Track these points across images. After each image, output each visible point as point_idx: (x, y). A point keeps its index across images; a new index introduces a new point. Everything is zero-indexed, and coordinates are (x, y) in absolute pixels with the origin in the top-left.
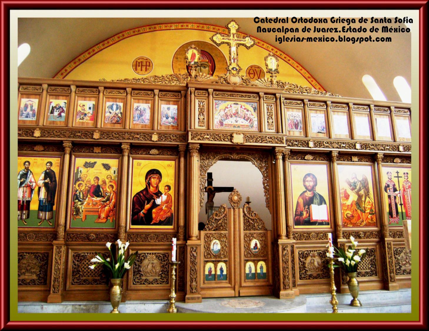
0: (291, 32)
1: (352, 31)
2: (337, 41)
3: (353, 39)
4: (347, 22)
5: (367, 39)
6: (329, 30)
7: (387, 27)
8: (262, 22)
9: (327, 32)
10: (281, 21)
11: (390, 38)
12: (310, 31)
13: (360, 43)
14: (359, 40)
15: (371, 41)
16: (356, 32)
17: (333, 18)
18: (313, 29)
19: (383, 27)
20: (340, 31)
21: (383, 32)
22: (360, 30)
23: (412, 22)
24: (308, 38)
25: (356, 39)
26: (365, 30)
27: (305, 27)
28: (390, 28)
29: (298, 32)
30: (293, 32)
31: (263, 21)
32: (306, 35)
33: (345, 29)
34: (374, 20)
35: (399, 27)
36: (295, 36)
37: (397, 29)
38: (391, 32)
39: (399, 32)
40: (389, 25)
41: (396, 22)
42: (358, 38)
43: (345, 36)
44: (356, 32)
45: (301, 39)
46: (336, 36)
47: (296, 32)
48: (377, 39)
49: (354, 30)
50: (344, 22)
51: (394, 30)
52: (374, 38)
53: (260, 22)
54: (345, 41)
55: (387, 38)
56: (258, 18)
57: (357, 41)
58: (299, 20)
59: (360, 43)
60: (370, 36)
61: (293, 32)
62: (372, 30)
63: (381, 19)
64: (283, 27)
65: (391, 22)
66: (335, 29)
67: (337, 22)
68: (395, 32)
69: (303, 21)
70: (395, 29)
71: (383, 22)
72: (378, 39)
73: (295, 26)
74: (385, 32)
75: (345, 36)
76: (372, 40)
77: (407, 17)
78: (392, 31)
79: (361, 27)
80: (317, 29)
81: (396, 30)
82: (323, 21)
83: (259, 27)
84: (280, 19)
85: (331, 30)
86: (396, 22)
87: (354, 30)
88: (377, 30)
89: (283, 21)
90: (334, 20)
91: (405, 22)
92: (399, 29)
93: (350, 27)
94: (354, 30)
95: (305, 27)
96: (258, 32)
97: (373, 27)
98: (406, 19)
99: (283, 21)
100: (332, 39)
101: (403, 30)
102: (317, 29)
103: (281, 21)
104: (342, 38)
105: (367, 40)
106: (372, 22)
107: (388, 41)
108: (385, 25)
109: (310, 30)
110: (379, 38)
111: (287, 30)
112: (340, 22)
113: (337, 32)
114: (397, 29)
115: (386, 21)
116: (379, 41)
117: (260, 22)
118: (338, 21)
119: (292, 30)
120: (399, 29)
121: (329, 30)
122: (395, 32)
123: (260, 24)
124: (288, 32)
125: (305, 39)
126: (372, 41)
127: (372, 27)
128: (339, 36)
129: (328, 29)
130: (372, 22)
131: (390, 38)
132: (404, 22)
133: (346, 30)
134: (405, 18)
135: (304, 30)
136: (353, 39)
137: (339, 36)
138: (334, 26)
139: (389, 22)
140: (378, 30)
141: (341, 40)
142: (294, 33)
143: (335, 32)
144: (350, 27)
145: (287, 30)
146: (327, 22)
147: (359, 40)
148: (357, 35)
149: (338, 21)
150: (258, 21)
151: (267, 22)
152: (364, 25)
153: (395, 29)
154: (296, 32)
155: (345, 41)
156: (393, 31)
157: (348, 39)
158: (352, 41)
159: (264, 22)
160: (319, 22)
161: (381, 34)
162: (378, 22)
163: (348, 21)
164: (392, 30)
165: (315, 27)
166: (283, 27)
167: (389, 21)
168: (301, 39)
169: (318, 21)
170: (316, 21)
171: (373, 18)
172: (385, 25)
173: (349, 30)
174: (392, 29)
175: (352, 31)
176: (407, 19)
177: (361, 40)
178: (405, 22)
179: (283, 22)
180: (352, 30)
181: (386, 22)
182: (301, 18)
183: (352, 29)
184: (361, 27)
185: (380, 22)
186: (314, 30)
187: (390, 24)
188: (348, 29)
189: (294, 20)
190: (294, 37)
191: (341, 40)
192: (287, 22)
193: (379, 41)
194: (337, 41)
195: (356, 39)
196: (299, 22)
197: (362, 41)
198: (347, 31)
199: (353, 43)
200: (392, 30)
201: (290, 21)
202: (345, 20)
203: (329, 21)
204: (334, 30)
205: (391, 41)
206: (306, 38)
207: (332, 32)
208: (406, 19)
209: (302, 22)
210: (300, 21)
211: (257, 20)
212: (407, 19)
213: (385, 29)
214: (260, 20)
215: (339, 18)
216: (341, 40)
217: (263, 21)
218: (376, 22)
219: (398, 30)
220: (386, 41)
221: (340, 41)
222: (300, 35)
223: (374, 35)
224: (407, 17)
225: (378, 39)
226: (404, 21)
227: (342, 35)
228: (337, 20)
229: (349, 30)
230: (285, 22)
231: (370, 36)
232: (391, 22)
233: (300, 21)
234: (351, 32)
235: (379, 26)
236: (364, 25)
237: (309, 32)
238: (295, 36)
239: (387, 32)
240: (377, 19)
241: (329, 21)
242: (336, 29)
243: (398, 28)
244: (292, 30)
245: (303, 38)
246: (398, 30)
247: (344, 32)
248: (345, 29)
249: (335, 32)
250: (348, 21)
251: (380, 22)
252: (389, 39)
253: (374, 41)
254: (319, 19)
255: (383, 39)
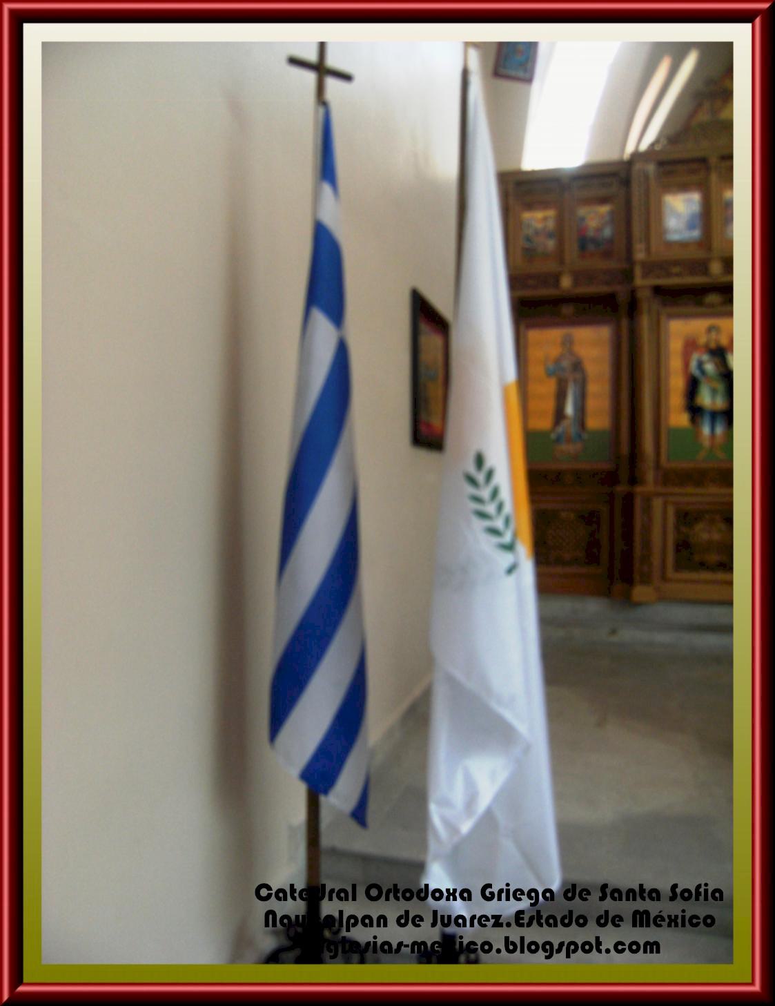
0: (365, 925)
1: (544, 924)
2: (499, 951)
3: (548, 947)
4: (531, 898)
5: (587, 947)
6: (476, 921)
7: (647, 913)
8: (279, 898)
9: (472, 925)
10: (334, 895)
11: (657, 944)
12: (421, 923)
13: (568, 956)
14: (564, 948)
15: (599, 951)
16: (556, 925)
17: (489, 886)
18: (429, 919)
19: (636, 913)
20: (509, 925)
21: (634, 925)
22: (567, 920)
23: (721, 899)
24: (414, 943)
25: (556, 947)
26: (582, 921)
27: (407, 912)
28: (657, 913)
29: (385, 925)
30: (371, 925)
31: (281, 895)
32: (409, 935)
33: (523, 919)
34: (608, 891)
35: (683, 911)
36: (375, 937)
37: (676, 917)
38: (660, 926)
39: (683, 925)
40: (653, 908)
41: (673, 898)
42: (561, 944)
43: (522, 939)
44: (556, 925)
45: (395, 946)
46: (497, 937)
47: (379, 925)
48: (619, 947)
49: (551, 921)
50: (520, 899)
51: (667, 920)
52: (608, 943)
53: (274, 894)
54: (522, 951)
55: (647, 943)
56: (269, 888)
57: (559, 951)
58: (389, 891)
59: (568, 956)
60: (597, 938)
61: (371, 925)
62: (602, 921)
63: (631, 891)
64: (341, 913)
65: (659, 899)
66: (493, 917)
67: (500, 899)
68: (669, 925)
69: (400, 895)
70: (669, 917)
71: (634, 899)
72: (620, 947)
73: (375, 910)
74: (641, 926)
75: (522, 939)
76: (603, 948)
77: (706, 885)
78: (662, 923)
79: (571, 912)
80: (442, 917)
81: (673, 921)
82: (457, 895)
83: (272, 913)
84: (332, 891)
85: (482, 920)
86: (673, 898)
87: (551, 921)
88: (617, 921)
89: (342, 895)
90: (491, 893)
91: (702, 898)
92: (683, 917)
93: (538, 912)
94: (552, 921)
95: (407, 912)
96: (267, 925)
97: (607, 912)
98: (702, 890)
99: (342, 895)
100: (486, 947)
101: (695, 921)
102: (442, 917)
103: (334, 895)
104: (513, 944)
105: (587, 948)
106: (602, 899)
107: (652, 952)
108: (640, 905)
109: (422, 920)
110: (623, 944)
111: (352, 921)
112: (508, 899)
113: (501, 925)
114: (676, 917)
115: (646, 895)
116: (622, 951)
117: (273, 895)
118: (504, 895)
119: (367, 921)
120: (683, 917)
121: (476, 921)
122: (669, 925)
123: (273, 904)
124: (355, 925)
125: (407, 946)
126: (603, 951)
127: (603, 913)
128: (507, 939)
129: (473, 917)
130: (602, 899)
131: (657, 944)
132: (697, 899)
133: (526, 921)
134: (699, 886)
135: (403, 921)
136: (548, 947)
137: (507, 939)
138: (491, 908)
139: (652, 899)
140: (621, 919)
141: (510, 946)
142: (374, 930)
143: (494, 926)
144: (538, 912)
145: (352, 921)
146: (470, 899)
147: (564, 948)
148: (556, 935)
149: (504, 895)
150: (269, 896)
151: (294, 898)
152: (577, 906)
153: (669, 917)
154: (379, 925)
155: (522, 951)
156: (665, 924)
157: (533, 948)
158: (545, 950)
159: (285, 899)
160: (448, 899)
161: (628, 933)
162: (621, 899)
163: (533, 894)
164: (663, 920)
165: (435, 913)
166: (341, 913)
167: (655, 894)
168: (395, 946)
169: (445, 894)
170: (437, 895)
171: (604, 886)
172: (640, 905)
173: (535, 922)
174: (661, 916)
175: (544, 924)
176: (706, 891)
177: (571, 948)
178: (702, 898)
179: (340, 899)
180: (543, 921)
181: (643, 899)
182: (395, 886)
183: (544, 918)
184: (571, 912)
185: (628, 899)
186: (431, 921)
187: (655, 903)
188: (531, 918)
189: (374, 892)
190: (372, 940)
191: (511, 947)
192: (354, 899)
193: (623, 951)
194: (499, 951)
195: (556, 947)
196: (387, 899)
197: (575, 951)
198: (529, 925)
199: (547, 958)
200: (663, 920)
201: (361, 891)
202: (523, 893)
203: (476, 894)
204: (492, 921)
205: (658, 952)
206: (408, 941)
207: (485, 926)
208: (702, 890)
209: (397, 898)
210: (391, 895)
211: (264, 892)
212: (706, 891)
213: (641, 919)
214: (273, 892)
215: (505, 888)
216: (511, 947)
217: (281, 895)
218: (614, 899)
219: (679, 921)
220: (645, 952)
221: (508, 951)
222: (393, 934)
223: (609, 936)
224: (706, 885)
225: (620, 947)
226: (698, 893)
227: (515, 934)
228: (501, 891)
229: (535, 922)
230: (347, 899)
231: (597, 938)
232: (659, 899)
233: (391, 895)
234: (541, 925)
235: (626, 908)
236: (577, 906)
237: (419, 926)
238: (375, 937)
239: (648, 925)
240: (617, 890)
241: (476, 894)
242: (496, 918)
243: (680, 914)
244: (367, 921)
245: (400, 944)
246: (679, 921)
247: (521, 925)
248: (523, 919)
249: (494, 926)
250: (533, 894)
251: (628, 899)
252: (653, 947)
253: (608, 951)
254: (448, 890)
255: (634, 948)
